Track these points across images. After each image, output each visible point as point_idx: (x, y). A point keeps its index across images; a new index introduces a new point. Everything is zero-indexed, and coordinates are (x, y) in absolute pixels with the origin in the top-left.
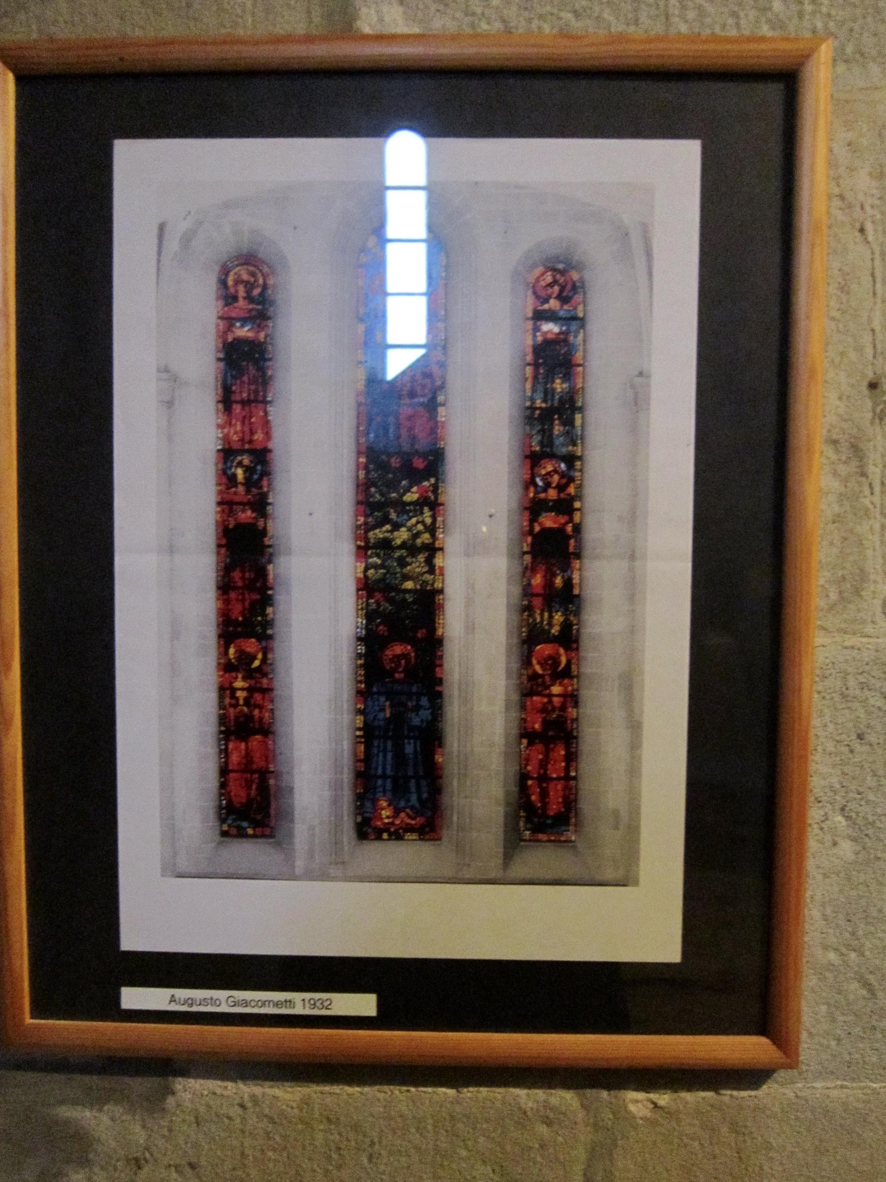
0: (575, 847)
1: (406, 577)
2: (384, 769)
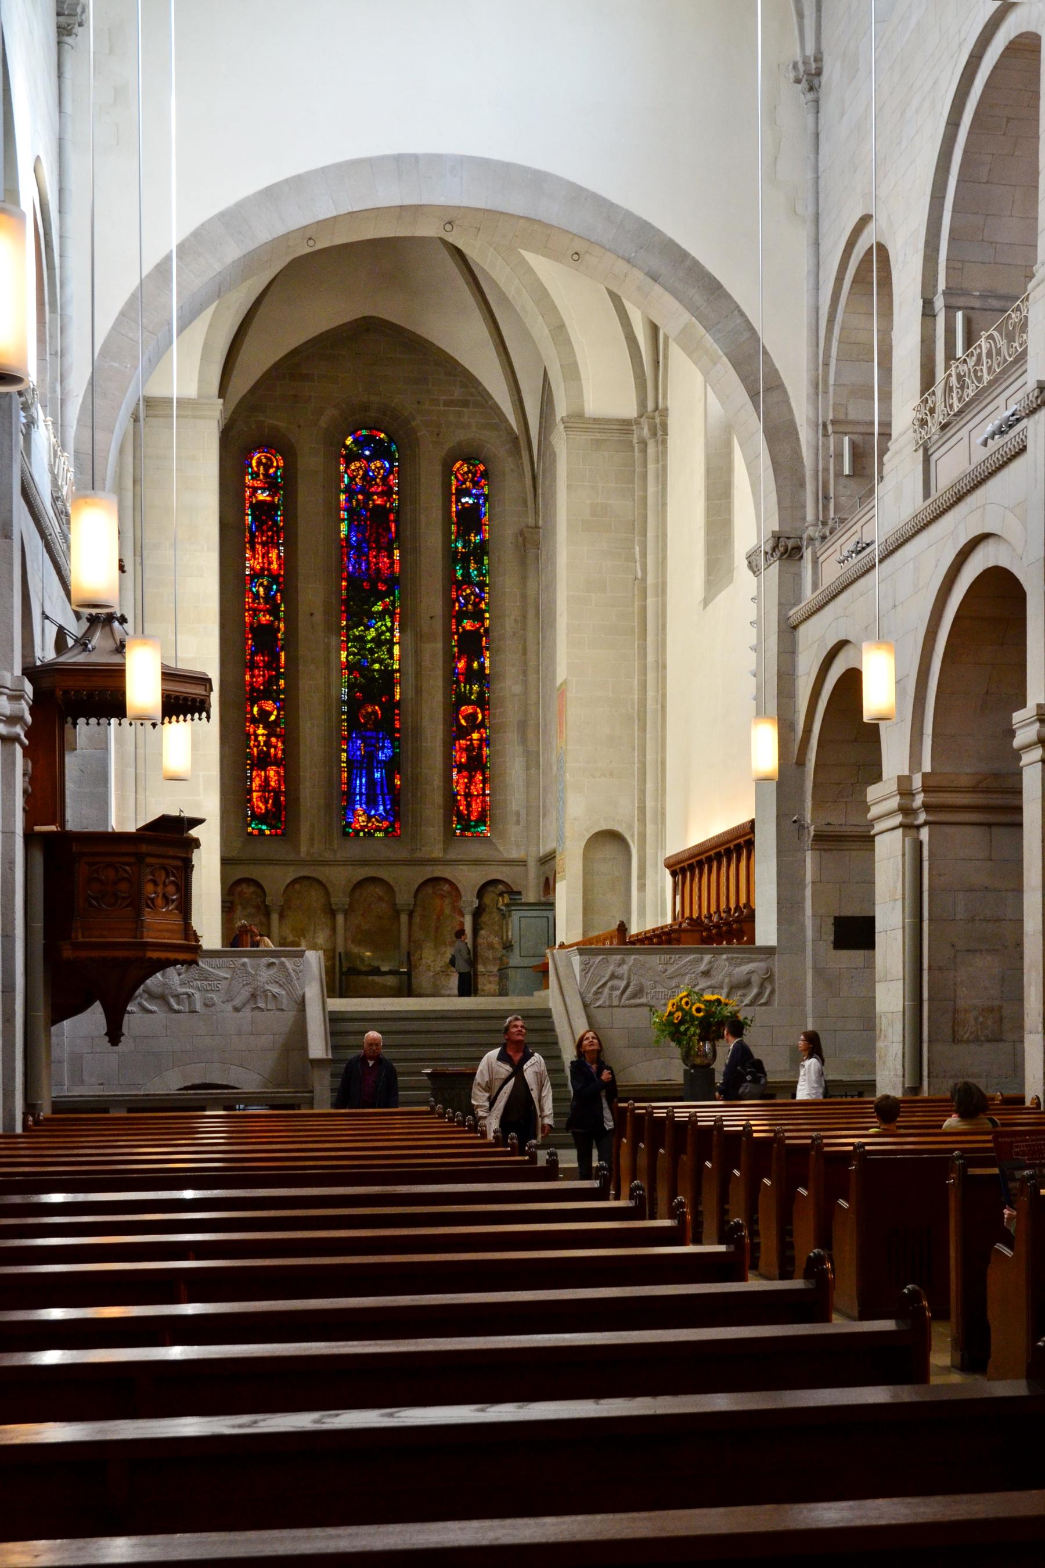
0: (491, 841)
1: (374, 661)
2: (361, 789)
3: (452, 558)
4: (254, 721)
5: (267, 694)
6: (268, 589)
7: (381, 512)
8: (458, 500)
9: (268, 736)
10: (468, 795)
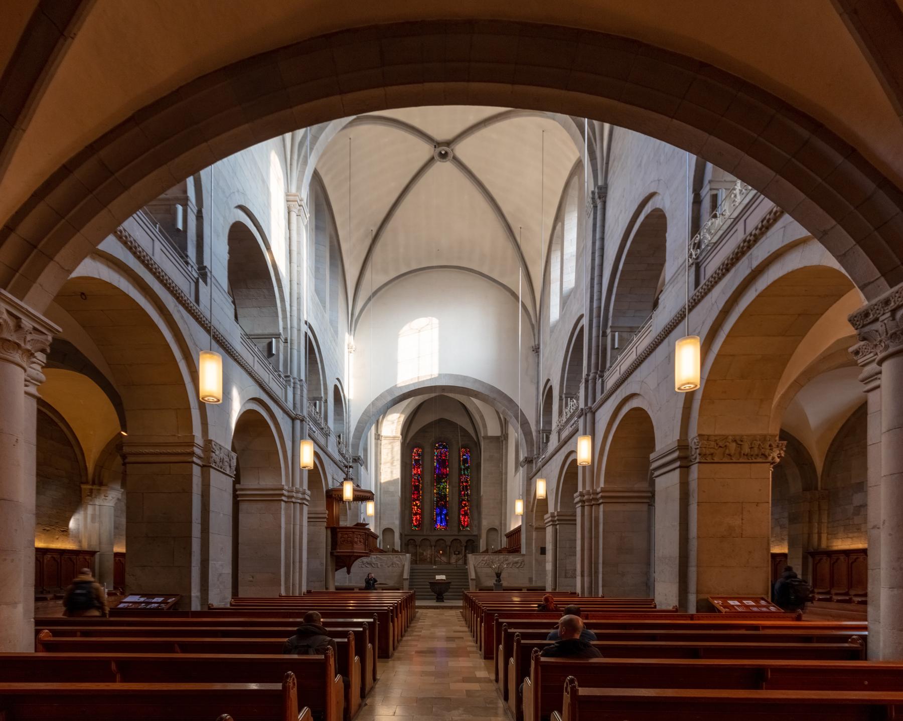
3: (460, 469)
7: (444, 461)
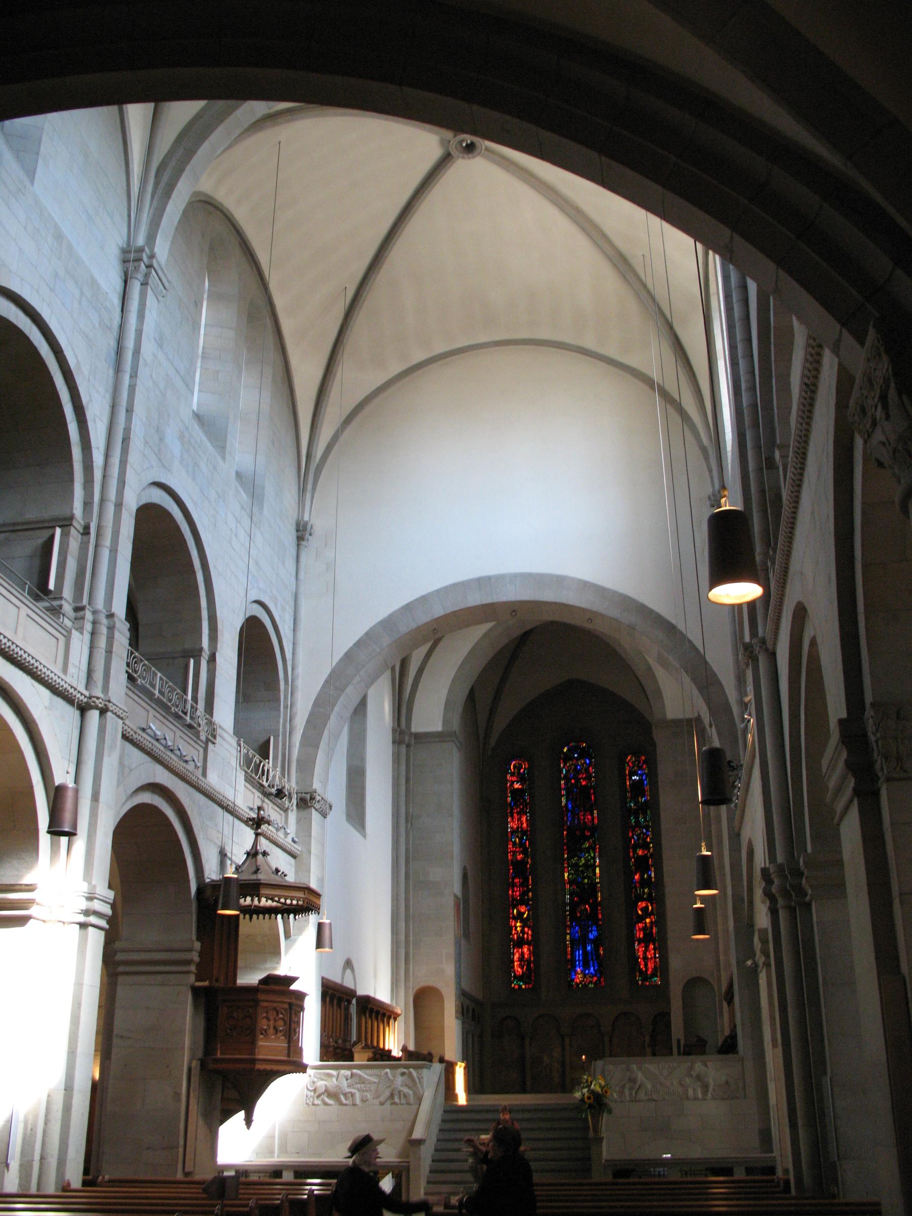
1: (585, 878)
4: (515, 918)
5: (522, 902)
6: (521, 839)
8: (630, 778)
9: (523, 927)
10: (645, 958)
